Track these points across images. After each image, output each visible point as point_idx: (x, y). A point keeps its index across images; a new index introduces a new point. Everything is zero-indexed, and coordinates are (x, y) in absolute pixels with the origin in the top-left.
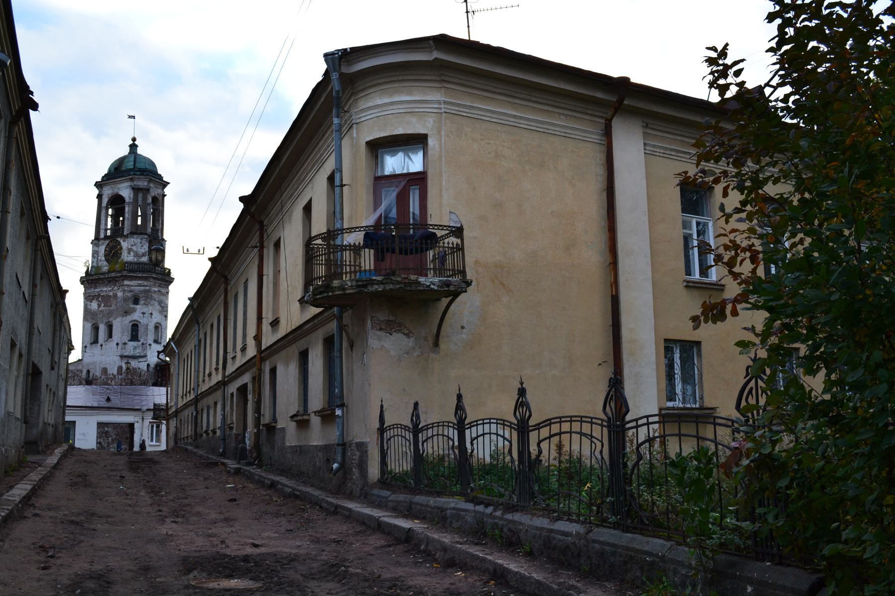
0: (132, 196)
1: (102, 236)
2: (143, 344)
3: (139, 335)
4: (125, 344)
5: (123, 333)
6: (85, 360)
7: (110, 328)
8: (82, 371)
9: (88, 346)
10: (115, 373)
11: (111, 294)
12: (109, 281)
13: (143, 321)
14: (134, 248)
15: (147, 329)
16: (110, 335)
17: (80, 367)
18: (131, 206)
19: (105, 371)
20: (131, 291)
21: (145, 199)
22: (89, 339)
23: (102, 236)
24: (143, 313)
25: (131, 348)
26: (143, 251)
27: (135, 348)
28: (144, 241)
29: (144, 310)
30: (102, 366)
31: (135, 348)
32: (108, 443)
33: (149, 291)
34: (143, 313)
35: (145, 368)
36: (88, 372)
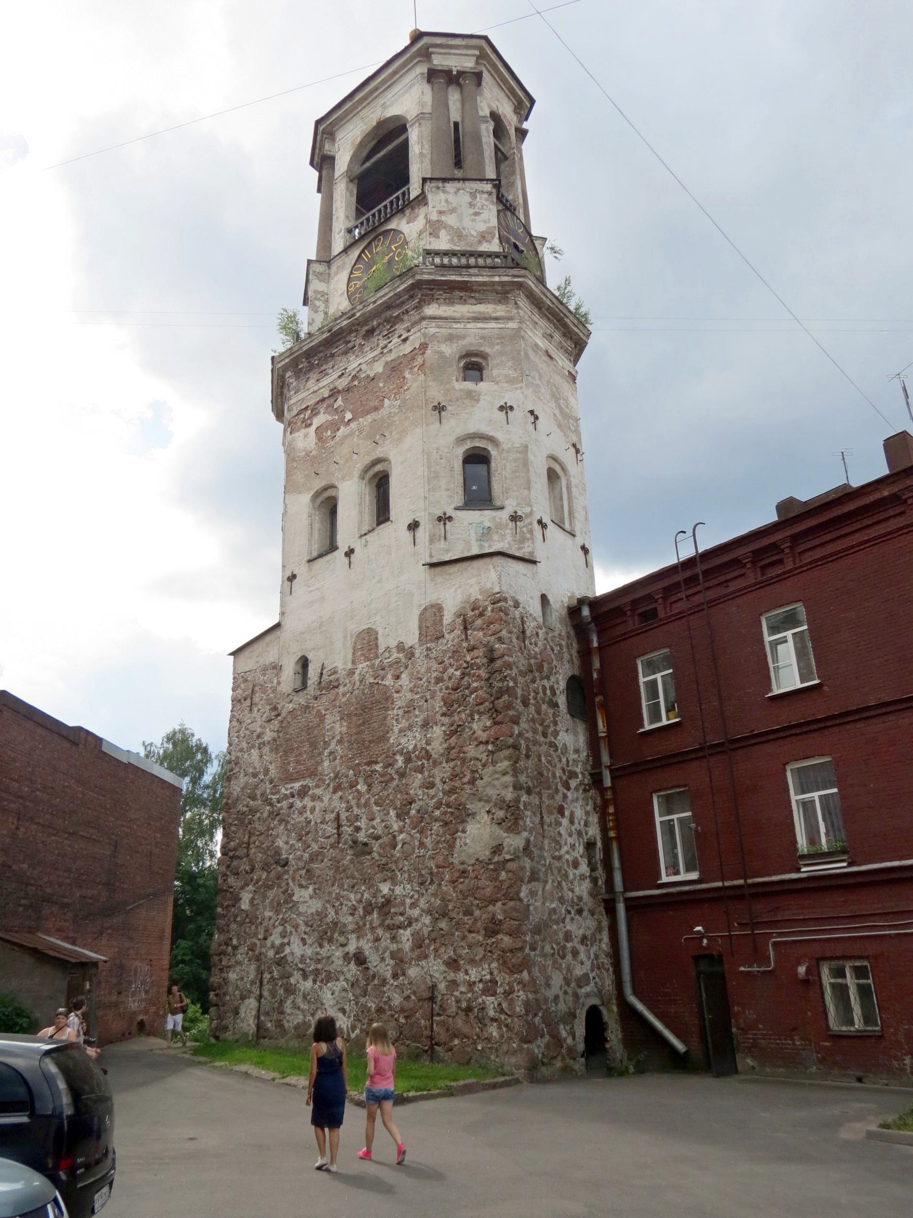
0: (428, 98)
1: (338, 245)
2: (515, 518)
3: (497, 487)
4: (444, 519)
5: (433, 478)
6: (287, 625)
7: (381, 484)
8: (277, 668)
9: (302, 570)
10: (411, 638)
11: (379, 368)
12: (370, 333)
13: (509, 435)
14: (451, 220)
15: (526, 463)
16: (382, 513)
17: (272, 656)
18: (427, 126)
19: (367, 642)
20: (451, 338)
21: (468, 102)
22: (306, 538)
23: (338, 245)
24: (506, 409)
25: (470, 529)
26: (482, 227)
27: (486, 534)
28: (482, 199)
29: (509, 398)
30: (355, 627)
31: (486, 534)
32: (400, 960)
33: (517, 335)
34: (506, 409)
35: (535, 608)
36: (304, 663)
